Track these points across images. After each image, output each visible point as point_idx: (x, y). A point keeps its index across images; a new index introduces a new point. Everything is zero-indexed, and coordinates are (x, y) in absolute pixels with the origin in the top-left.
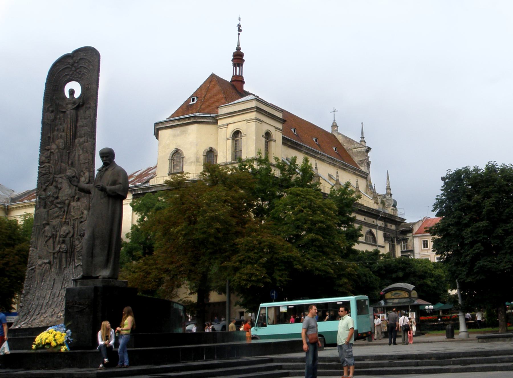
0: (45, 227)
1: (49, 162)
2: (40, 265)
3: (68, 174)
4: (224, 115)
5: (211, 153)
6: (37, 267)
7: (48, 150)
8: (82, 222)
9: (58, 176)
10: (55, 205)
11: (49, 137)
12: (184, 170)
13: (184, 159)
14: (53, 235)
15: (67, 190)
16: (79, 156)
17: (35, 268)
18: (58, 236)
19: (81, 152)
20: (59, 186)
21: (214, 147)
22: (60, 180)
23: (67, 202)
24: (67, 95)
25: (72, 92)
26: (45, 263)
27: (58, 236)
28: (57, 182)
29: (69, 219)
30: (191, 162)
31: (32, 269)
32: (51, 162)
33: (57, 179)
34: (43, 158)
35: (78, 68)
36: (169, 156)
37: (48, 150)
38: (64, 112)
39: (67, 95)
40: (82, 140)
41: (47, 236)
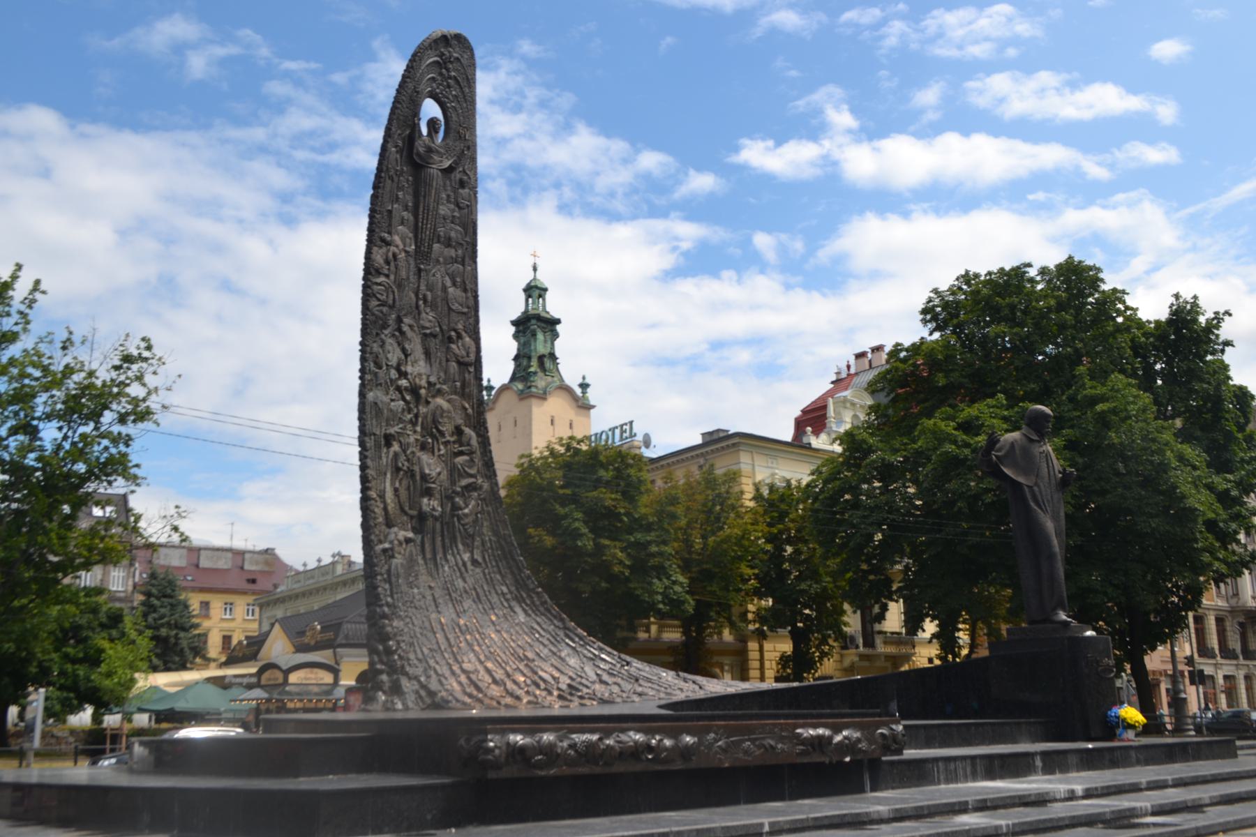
1: (387, 276)
2: (400, 543)
3: (428, 325)
6: (397, 549)
8: (461, 453)
10: (401, 392)
11: (390, 212)
15: (422, 363)
16: (444, 289)
17: (392, 549)
19: (448, 283)
23: (423, 392)
26: (408, 541)
28: (402, 333)
31: (385, 551)
32: (392, 277)
33: (405, 328)
35: (450, 78)
41: (398, 469)
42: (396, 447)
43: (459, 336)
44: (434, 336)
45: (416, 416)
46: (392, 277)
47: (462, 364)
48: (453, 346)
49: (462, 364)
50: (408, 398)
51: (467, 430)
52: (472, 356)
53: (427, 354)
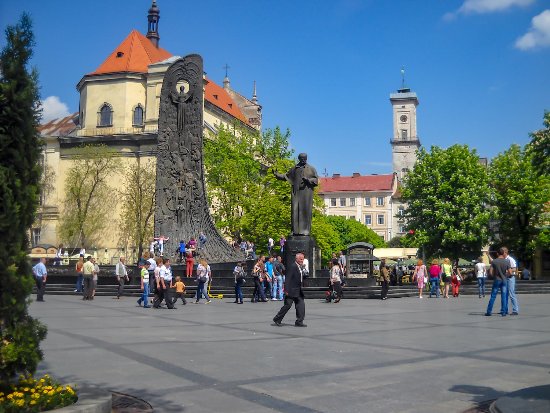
0: (165, 191)
4: (155, 73)
5: (139, 110)
7: (165, 132)
9: (174, 152)
12: (113, 123)
13: (113, 113)
14: (173, 197)
18: (177, 198)
19: (191, 136)
20: (174, 160)
21: (143, 104)
22: (175, 156)
23: (181, 173)
24: (179, 91)
25: (182, 89)
26: (169, 218)
27: (177, 198)
28: (172, 157)
29: (184, 186)
30: (121, 117)
34: (162, 138)
36: (98, 109)
37: (165, 132)
38: (177, 104)
39: (179, 91)
40: (193, 125)
41: (168, 198)
42: (168, 191)
43: (195, 152)
44: (186, 154)
45: (179, 180)
46: (168, 141)
47: (196, 161)
48: (193, 156)
49: (196, 161)
50: (174, 175)
51: (199, 182)
52: (199, 158)
53: (183, 160)
